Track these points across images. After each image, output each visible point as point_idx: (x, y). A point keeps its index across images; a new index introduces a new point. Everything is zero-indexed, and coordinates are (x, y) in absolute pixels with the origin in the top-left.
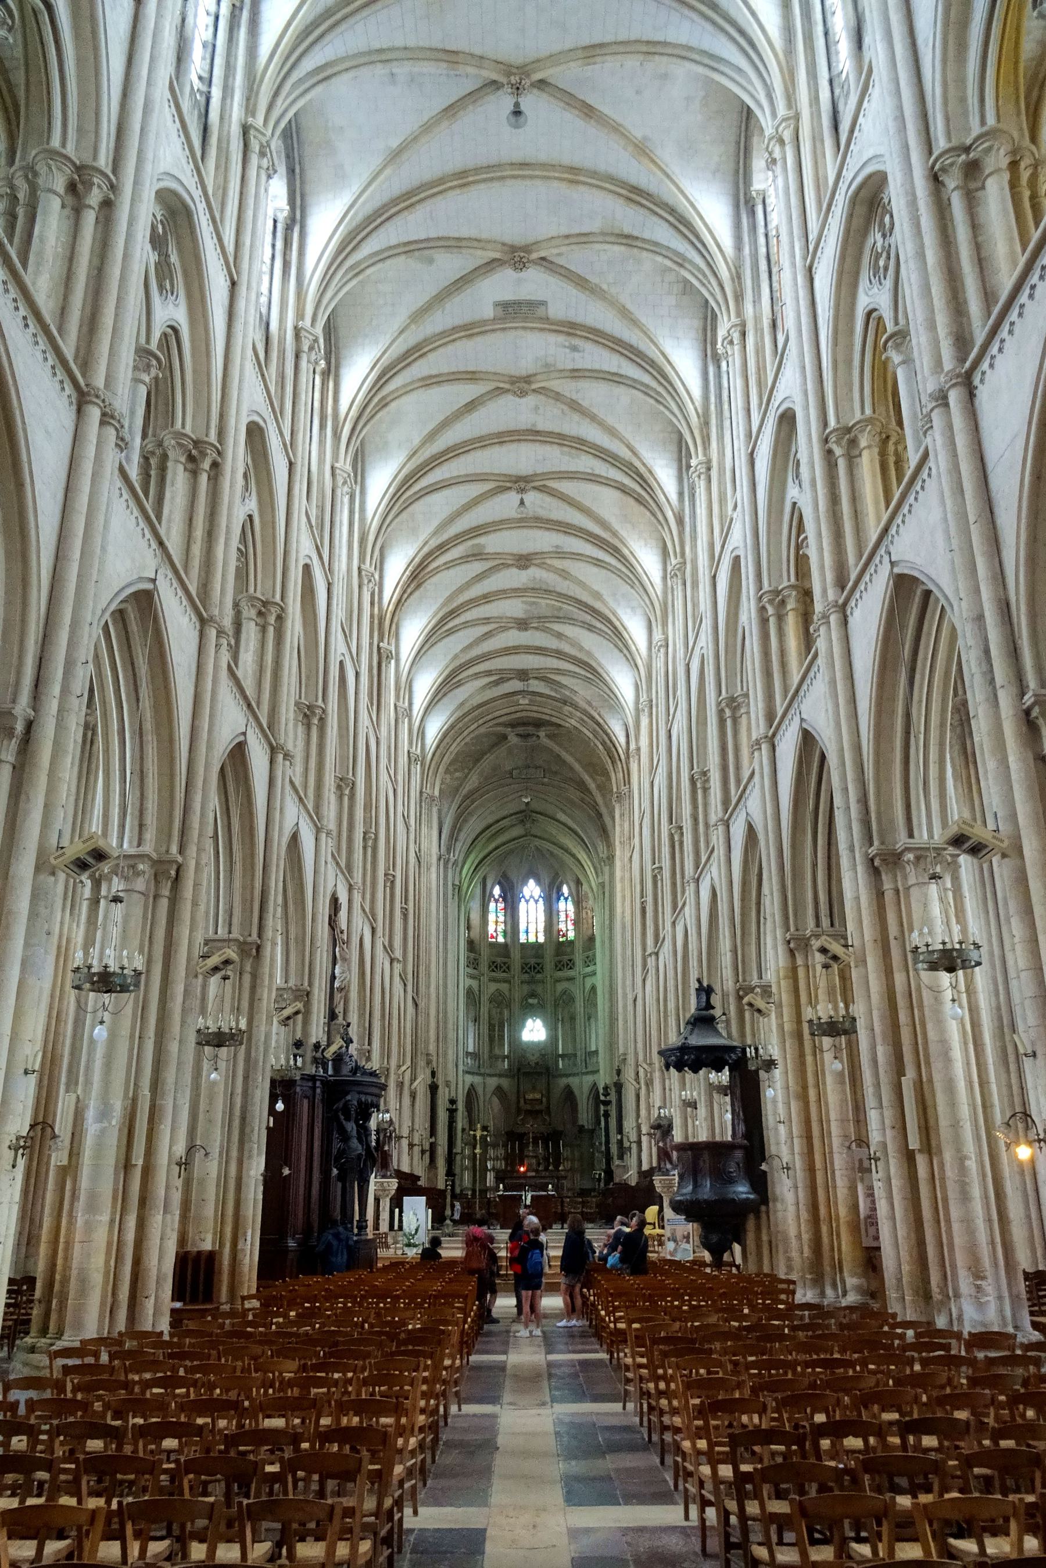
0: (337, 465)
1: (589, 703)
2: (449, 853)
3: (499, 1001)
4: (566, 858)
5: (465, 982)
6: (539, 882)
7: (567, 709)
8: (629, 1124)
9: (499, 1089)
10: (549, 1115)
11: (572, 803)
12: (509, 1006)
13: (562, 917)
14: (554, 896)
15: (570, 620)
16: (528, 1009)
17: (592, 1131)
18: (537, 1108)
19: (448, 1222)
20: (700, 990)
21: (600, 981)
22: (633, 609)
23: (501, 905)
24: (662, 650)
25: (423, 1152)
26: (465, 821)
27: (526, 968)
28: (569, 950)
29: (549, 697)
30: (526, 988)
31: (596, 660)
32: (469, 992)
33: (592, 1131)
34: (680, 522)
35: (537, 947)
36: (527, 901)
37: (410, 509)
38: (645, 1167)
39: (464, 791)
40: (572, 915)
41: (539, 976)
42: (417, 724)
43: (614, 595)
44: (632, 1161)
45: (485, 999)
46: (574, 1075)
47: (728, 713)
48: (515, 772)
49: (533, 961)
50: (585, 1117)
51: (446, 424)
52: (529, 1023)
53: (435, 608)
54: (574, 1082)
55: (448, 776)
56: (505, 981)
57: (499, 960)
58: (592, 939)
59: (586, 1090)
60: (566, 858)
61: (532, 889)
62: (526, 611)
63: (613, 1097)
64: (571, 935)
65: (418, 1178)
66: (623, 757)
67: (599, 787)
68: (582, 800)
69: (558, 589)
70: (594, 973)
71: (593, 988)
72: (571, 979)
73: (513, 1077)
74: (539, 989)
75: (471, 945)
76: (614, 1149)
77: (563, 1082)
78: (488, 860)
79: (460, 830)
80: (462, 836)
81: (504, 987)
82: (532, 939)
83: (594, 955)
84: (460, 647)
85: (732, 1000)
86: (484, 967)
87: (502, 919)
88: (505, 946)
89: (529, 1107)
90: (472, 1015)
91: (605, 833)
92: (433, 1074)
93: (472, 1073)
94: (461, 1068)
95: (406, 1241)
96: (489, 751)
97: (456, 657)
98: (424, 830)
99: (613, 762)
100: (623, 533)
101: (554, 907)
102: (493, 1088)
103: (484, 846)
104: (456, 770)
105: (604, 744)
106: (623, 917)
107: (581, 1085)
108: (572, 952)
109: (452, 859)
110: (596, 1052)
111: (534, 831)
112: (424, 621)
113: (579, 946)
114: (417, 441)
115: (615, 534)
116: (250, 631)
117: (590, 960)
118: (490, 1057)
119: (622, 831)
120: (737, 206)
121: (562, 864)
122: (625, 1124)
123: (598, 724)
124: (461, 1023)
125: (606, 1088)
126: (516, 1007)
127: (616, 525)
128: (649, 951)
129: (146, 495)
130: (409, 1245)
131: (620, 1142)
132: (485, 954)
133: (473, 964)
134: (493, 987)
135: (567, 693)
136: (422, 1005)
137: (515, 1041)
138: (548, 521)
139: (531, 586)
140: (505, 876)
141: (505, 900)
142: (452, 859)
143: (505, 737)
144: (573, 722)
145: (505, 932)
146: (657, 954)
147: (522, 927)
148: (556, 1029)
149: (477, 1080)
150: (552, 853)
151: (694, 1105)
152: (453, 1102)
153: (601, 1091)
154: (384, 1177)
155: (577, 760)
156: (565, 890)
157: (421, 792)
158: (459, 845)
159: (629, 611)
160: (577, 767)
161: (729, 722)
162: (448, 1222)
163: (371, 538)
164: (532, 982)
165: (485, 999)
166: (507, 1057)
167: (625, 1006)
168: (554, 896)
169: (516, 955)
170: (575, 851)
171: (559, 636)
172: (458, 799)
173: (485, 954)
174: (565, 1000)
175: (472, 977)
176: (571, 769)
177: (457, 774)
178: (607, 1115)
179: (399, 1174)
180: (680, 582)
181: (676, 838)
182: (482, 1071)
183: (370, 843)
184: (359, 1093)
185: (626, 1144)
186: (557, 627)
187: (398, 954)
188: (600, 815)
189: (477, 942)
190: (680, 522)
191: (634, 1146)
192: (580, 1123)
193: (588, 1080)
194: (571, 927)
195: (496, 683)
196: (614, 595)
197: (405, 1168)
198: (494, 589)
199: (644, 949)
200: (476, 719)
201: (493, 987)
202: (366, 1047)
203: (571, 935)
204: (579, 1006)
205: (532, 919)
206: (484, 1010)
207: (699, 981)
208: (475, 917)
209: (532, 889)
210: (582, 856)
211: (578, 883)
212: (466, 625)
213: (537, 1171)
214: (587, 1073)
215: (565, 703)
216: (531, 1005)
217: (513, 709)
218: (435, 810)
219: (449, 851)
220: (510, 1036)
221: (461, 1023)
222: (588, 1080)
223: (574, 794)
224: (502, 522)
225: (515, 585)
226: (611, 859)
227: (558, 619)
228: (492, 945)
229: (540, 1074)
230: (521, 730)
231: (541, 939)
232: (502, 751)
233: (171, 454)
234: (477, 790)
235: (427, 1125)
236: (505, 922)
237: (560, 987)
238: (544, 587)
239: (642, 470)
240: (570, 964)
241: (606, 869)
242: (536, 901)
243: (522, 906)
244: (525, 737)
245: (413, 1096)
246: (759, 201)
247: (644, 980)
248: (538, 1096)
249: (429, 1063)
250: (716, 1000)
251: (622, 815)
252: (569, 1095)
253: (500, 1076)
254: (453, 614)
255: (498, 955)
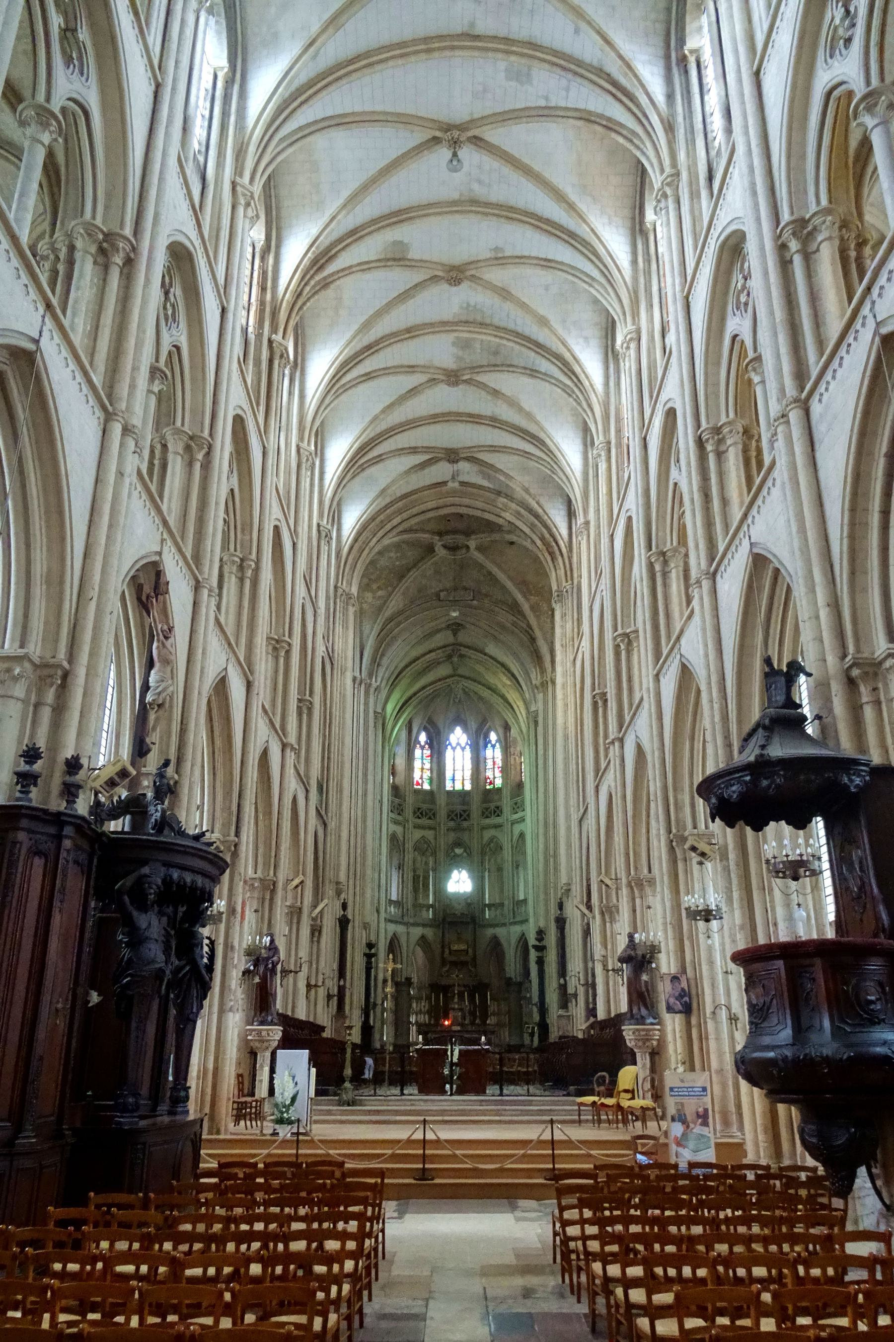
0: (238, 180)
1: (527, 490)
2: (371, 678)
3: (422, 848)
4: (496, 700)
5: (388, 828)
6: (466, 729)
7: (502, 500)
8: (575, 965)
9: (423, 937)
10: (475, 966)
11: (503, 627)
12: (434, 854)
13: (490, 764)
14: (481, 743)
15: (509, 367)
16: (454, 861)
17: (520, 984)
18: (463, 958)
19: (347, 1085)
20: (771, 673)
21: (528, 827)
22: (586, 339)
23: (427, 752)
24: (633, 345)
25: (329, 997)
26: (389, 645)
27: (452, 815)
28: (496, 797)
29: (481, 487)
30: (452, 836)
31: (537, 423)
32: (393, 838)
33: (520, 984)
34: (670, 128)
35: (463, 794)
36: (454, 749)
37: (309, 139)
38: (601, 1015)
39: (388, 613)
40: (499, 762)
41: (465, 824)
42: (329, 494)
43: (564, 321)
44: (578, 1010)
45: (409, 846)
46: (504, 925)
47: (794, 245)
48: (442, 594)
49: (459, 808)
50: (512, 969)
51: (379, 314)
52: (455, 874)
53: (348, 335)
54: (500, 932)
55: (369, 596)
56: (430, 828)
57: (425, 807)
58: (520, 785)
59: (514, 941)
60: (496, 700)
61: (458, 736)
62: (459, 359)
63: (551, 940)
64: (498, 783)
65: (323, 1029)
66: (564, 550)
67: (532, 608)
68: (514, 624)
69: (496, 322)
70: (523, 820)
71: (522, 835)
72: (498, 826)
73: (438, 927)
74: (465, 837)
75: (395, 790)
76: (552, 997)
77: (490, 932)
78: (414, 702)
79: (383, 655)
80: (385, 661)
81: (430, 834)
82: (458, 787)
83: (523, 801)
84: (380, 407)
85: (837, 689)
86: (409, 812)
87: (427, 766)
88: (431, 793)
89: (453, 958)
90: (395, 862)
91: (537, 657)
92: (344, 906)
93: (396, 922)
94: (383, 915)
95: (277, 1115)
96: (415, 565)
97: (375, 418)
98: (339, 629)
99: (553, 559)
100: (582, 206)
101: (482, 754)
102: (417, 938)
103: (410, 685)
104: (379, 588)
105: (542, 539)
106: (566, 728)
107: (509, 935)
108: (500, 799)
109: (374, 685)
110: (525, 901)
111: (460, 671)
112: (335, 351)
113: (506, 793)
114: (315, 28)
115: (571, 207)
116: (176, 467)
117: (518, 806)
118: (415, 906)
119: (564, 635)
120: (668, 69)
121: (490, 707)
122: (570, 967)
123: (537, 516)
124: (384, 869)
125: (541, 934)
126: (441, 855)
127: (573, 196)
128: (611, 737)
129: (53, 293)
130: (280, 1121)
131: (563, 988)
132: (410, 802)
133: (398, 809)
134: (418, 834)
135: (502, 478)
136: (332, 825)
137: (440, 891)
138: (487, 204)
139: (464, 318)
140: (431, 721)
141: (431, 747)
142: (374, 685)
143: (430, 550)
144: (508, 516)
145: (431, 779)
146: (621, 740)
147: (449, 774)
148: (483, 877)
149: (401, 929)
150: (480, 698)
151: (707, 915)
152: (370, 946)
153: (532, 941)
154: (262, 1023)
155: (510, 578)
156: (493, 736)
157: (336, 587)
158: (381, 671)
159: (581, 341)
160: (509, 585)
161: (797, 260)
162: (347, 1085)
163: (309, 418)
164: (458, 829)
165: (409, 846)
166: (432, 906)
167: (569, 828)
168: (481, 743)
169: (442, 801)
170: (504, 691)
171: (496, 393)
172: (381, 620)
173: (410, 800)
174: (494, 847)
175: (396, 822)
176: (503, 588)
177: (380, 593)
178: (540, 962)
179: (287, 1021)
180: (670, 200)
181: (658, 567)
182: (406, 919)
183: (249, 573)
184: (168, 865)
185: (571, 990)
186: (491, 379)
187: (292, 739)
188: (533, 640)
189: (402, 788)
190: (670, 128)
191: (581, 991)
192: (508, 975)
193: (516, 930)
194: (498, 774)
195: (423, 466)
196: (564, 321)
197: (301, 1014)
198: (419, 320)
199: (606, 736)
200: (400, 512)
201: (418, 834)
202: (232, 837)
203: (498, 783)
204: (507, 853)
205: (458, 766)
206: (409, 857)
207: (768, 661)
208: (400, 762)
209: (458, 736)
210: (512, 696)
211: (507, 728)
212: (386, 371)
213: (461, 1025)
214: (515, 923)
215: (499, 493)
216: (458, 856)
217: (441, 502)
218: (351, 610)
219: (370, 675)
220: (434, 885)
221: (384, 869)
222: (516, 930)
223: (505, 617)
224: (430, 205)
225: (447, 316)
226: (547, 685)
227: (494, 367)
228: (417, 792)
229: (467, 923)
230: (449, 539)
231: (468, 787)
232: (427, 567)
233: (79, 244)
234: (400, 613)
235: (335, 966)
236: (431, 770)
237: (488, 834)
238: (479, 318)
239: (567, 356)
240: (498, 811)
241: (540, 696)
242: (463, 749)
243: (449, 753)
244: (453, 549)
245: (316, 931)
246: (692, 60)
247: (597, 788)
248: (463, 947)
249: (338, 893)
250: (803, 689)
251: (564, 616)
252: (496, 944)
253: (424, 925)
254: (370, 349)
255: (424, 802)
